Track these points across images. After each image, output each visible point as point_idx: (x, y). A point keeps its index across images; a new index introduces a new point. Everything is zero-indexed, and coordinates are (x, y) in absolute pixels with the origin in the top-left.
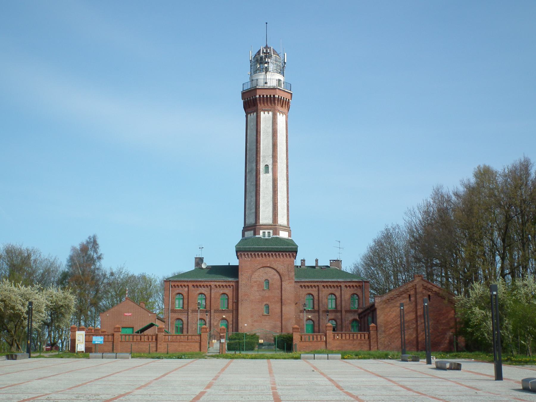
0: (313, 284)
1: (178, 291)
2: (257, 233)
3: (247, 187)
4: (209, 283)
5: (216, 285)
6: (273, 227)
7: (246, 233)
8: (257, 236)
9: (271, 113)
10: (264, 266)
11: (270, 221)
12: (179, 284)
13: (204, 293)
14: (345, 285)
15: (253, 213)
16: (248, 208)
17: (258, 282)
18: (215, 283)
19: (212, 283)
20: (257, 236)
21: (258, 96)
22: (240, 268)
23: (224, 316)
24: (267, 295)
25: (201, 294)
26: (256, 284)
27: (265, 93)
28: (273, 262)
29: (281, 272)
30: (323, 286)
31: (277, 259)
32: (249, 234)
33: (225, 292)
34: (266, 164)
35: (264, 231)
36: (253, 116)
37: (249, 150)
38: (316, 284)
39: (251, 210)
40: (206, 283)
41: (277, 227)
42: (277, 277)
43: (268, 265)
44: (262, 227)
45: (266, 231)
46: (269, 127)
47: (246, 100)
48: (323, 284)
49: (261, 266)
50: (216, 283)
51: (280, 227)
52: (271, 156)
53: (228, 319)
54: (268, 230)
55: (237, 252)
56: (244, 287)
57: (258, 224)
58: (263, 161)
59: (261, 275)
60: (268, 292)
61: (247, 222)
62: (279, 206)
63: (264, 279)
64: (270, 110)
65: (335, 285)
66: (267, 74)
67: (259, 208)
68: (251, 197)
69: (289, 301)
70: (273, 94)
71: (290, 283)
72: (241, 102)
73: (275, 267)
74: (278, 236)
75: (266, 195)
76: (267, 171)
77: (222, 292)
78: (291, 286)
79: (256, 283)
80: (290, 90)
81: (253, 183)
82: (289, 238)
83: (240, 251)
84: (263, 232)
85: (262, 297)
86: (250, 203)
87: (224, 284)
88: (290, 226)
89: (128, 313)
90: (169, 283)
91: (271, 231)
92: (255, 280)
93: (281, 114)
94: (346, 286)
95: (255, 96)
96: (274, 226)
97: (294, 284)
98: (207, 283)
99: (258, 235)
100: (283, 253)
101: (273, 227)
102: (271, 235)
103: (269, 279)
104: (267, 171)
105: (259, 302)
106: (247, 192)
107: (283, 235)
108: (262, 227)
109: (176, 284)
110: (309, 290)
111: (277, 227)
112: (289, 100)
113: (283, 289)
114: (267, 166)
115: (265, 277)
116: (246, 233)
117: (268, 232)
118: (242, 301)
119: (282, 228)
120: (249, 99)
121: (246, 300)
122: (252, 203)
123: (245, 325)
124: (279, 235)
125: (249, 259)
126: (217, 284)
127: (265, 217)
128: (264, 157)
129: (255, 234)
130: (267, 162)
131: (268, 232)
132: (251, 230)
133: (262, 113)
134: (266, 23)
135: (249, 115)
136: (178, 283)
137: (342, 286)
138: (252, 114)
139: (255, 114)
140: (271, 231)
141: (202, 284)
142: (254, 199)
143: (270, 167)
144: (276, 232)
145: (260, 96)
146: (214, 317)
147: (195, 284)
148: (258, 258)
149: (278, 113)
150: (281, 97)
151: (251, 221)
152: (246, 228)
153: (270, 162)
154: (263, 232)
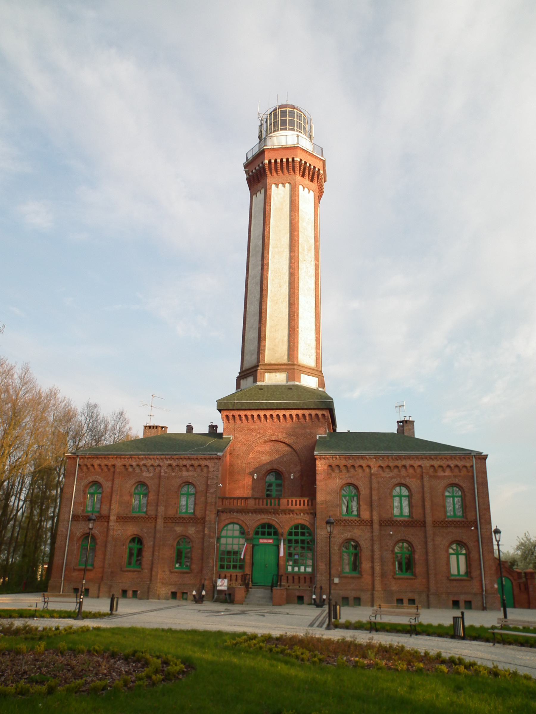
8: (259, 383)
21: (266, 161)
32: (248, 383)
36: (260, 196)
41: (296, 367)
47: (250, 174)
57: (260, 363)
62: (252, 256)
72: (244, 176)
74: (296, 383)
80: (322, 156)
82: (320, 389)
93: (306, 189)
95: (262, 163)
99: (260, 381)
111: (296, 367)
112: (319, 170)
120: (254, 171)
124: (300, 382)
129: (255, 381)
133: (273, 186)
135: (254, 197)
138: (258, 194)
145: (270, 161)
149: (301, 187)
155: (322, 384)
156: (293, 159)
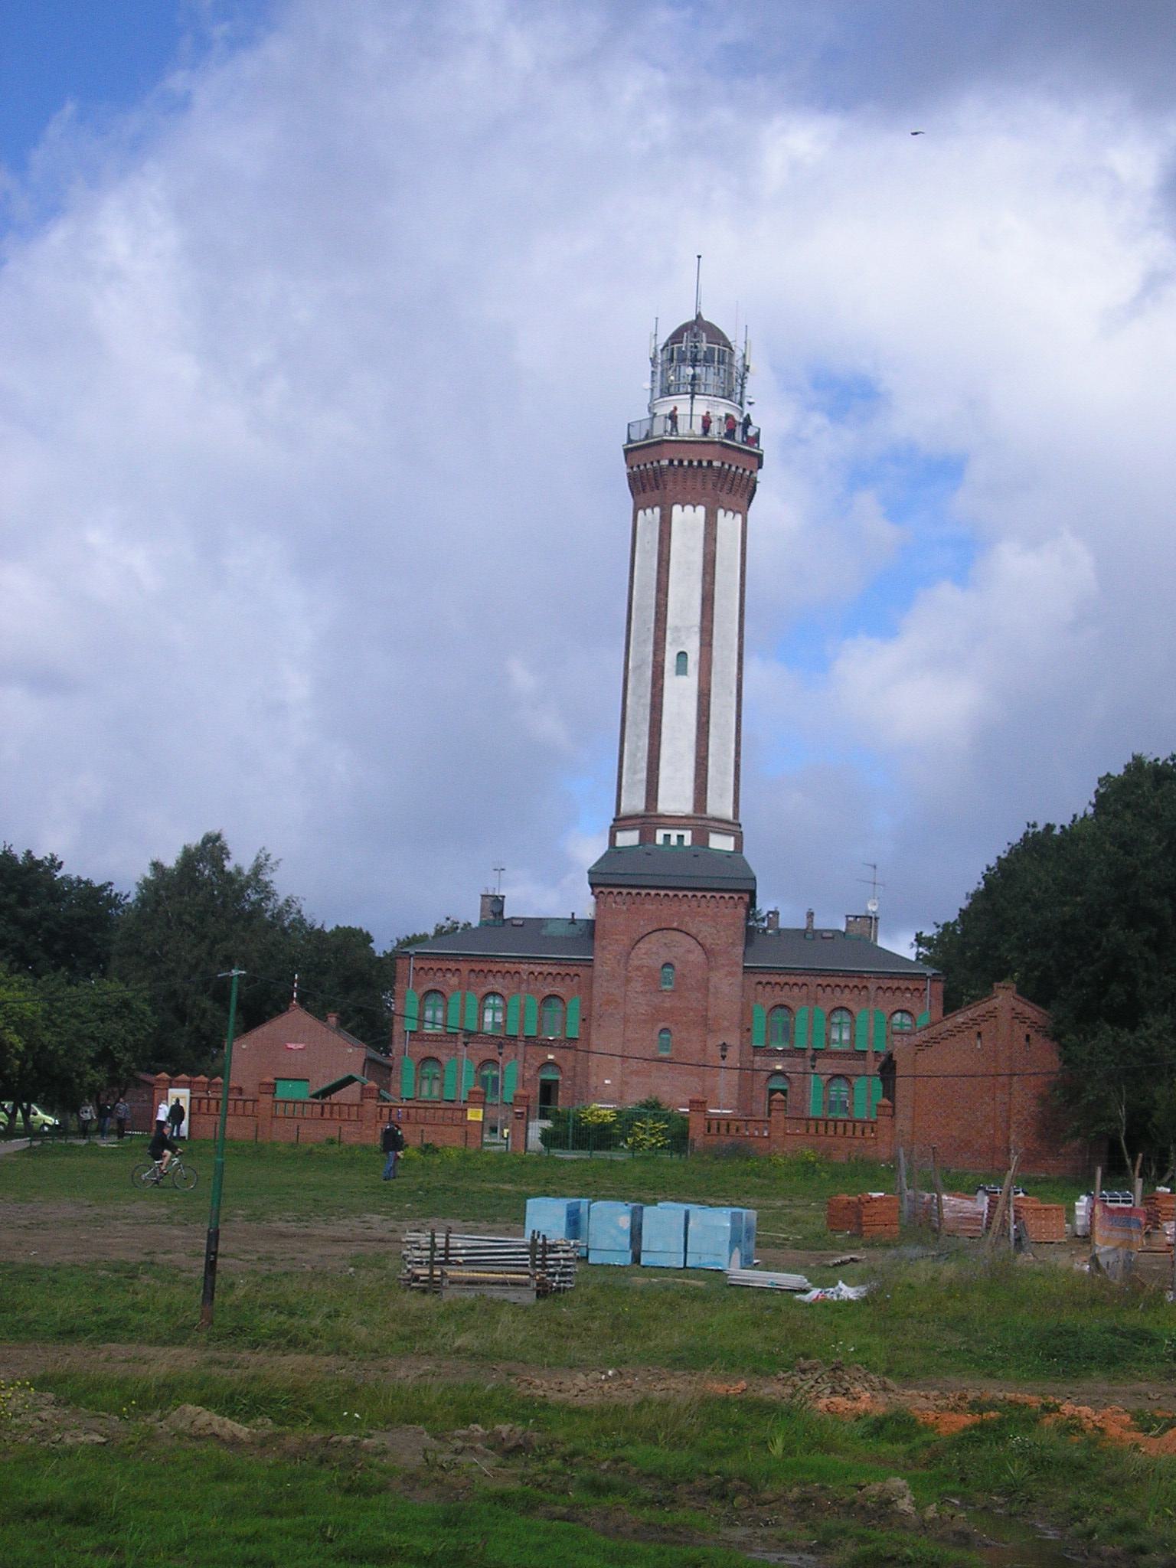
0: (792, 980)
1: (431, 986)
3: (628, 710)
4: (517, 965)
5: (532, 973)
7: (619, 835)
9: (701, 510)
10: (663, 925)
12: (435, 965)
13: (499, 991)
14: (877, 986)
15: (640, 781)
17: (645, 969)
18: (531, 965)
19: (522, 966)
21: (665, 462)
22: (598, 927)
23: (551, 1057)
24: (667, 1005)
25: (493, 994)
26: (639, 974)
27: (687, 456)
28: (687, 919)
29: (708, 942)
30: (819, 985)
31: (699, 909)
32: (628, 838)
33: (555, 993)
34: (682, 650)
35: (667, 832)
37: (636, 609)
39: (635, 773)
40: (506, 965)
42: (698, 956)
43: (675, 925)
44: (662, 820)
45: (674, 834)
47: (635, 469)
48: (819, 981)
49: (655, 926)
50: (532, 968)
51: (712, 824)
52: (697, 629)
53: (560, 1062)
54: (678, 829)
55: (592, 885)
56: (608, 981)
58: (674, 640)
59: (654, 950)
60: (669, 996)
61: (622, 805)
63: (661, 962)
64: (699, 504)
65: (851, 985)
66: (694, 401)
67: (658, 769)
68: (638, 736)
69: (726, 1024)
70: (709, 458)
71: (730, 974)
73: (693, 931)
76: (681, 669)
77: (547, 992)
78: (730, 985)
79: (640, 971)
81: (642, 701)
83: (601, 880)
84: (665, 835)
85: (655, 1008)
86: (633, 755)
87: (554, 970)
88: (741, 821)
90: (407, 962)
92: (637, 963)
93: (730, 514)
94: (880, 988)
95: (658, 462)
96: (701, 822)
97: (741, 977)
98: (512, 965)
100: (714, 894)
101: (693, 822)
102: (687, 842)
103: (677, 964)
104: (681, 669)
105: (645, 1021)
106: (628, 724)
107: (721, 843)
108: (662, 820)
109: (427, 965)
110: (781, 996)
113: (712, 990)
114: (682, 655)
115: (665, 956)
116: (619, 835)
117: (678, 836)
118: (601, 1017)
119: (717, 824)
121: (612, 1015)
122: (639, 755)
123: (607, 1082)
125: (625, 908)
126: (537, 969)
127: (676, 798)
128: (677, 629)
130: (683, 644)
131: (678, 836)
132: (632, 828)
133: (677, 509)
134: (699, 257)
135: (641, 513)
136: (433, 962)
137: (870, 989)
138: (648, 511)
139: (657, 510)
140: (688, 835)
141: (495, 968)
142: (645, 742)
144: (701, 838)
145: (671, 462)
146: (525, 1058)
147: (477, 967)
148: (648, 907)
149: (721, 512)
150: (730, 466)
151: (634, 803)
152: (621, 822)
153: (693, 648)
154: (665, 835)
155: (739, 845)
156: (710, 463)
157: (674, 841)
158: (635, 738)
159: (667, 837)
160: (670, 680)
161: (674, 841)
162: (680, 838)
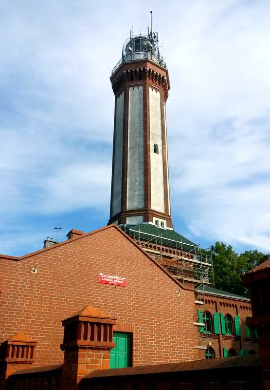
2: (150, 219)
6: (166, 217)
8: (150, 223)
11: (162, 210)
16: (130, 189)
20: (150, 223)
37: (131, 125)
38: (214, 299)
39: (135, 192)
44: (154, 213)
45: (160, 220)
46: (157, 106)
52: (160, 137)
67: (150, 190)
75: (156, 178)
89: (113, 274)
91: (165, 222)
104: (156, 151)
114: (156, 146)
127: (157, 205)
128: (153, 134)
129: (146, 219)
130: (156, 141)
132: (139, 215)
140: (165, 222)
143: (160, 148)
157: (160, 223)
158: (134, 176)
159: (157, 222)
160: (152, 154)
161: (160, 223)
162: (162, 223)
